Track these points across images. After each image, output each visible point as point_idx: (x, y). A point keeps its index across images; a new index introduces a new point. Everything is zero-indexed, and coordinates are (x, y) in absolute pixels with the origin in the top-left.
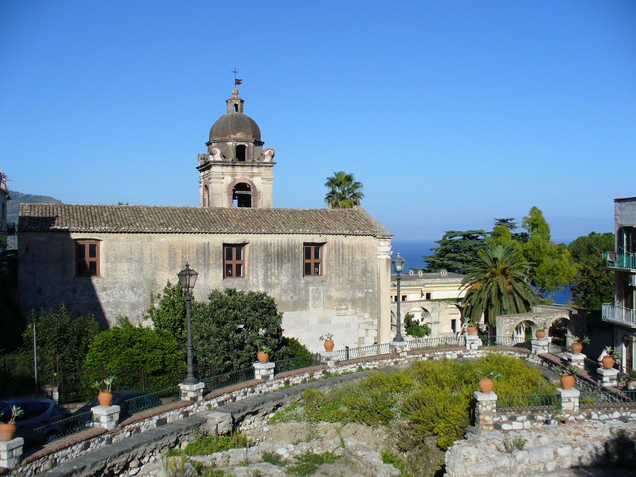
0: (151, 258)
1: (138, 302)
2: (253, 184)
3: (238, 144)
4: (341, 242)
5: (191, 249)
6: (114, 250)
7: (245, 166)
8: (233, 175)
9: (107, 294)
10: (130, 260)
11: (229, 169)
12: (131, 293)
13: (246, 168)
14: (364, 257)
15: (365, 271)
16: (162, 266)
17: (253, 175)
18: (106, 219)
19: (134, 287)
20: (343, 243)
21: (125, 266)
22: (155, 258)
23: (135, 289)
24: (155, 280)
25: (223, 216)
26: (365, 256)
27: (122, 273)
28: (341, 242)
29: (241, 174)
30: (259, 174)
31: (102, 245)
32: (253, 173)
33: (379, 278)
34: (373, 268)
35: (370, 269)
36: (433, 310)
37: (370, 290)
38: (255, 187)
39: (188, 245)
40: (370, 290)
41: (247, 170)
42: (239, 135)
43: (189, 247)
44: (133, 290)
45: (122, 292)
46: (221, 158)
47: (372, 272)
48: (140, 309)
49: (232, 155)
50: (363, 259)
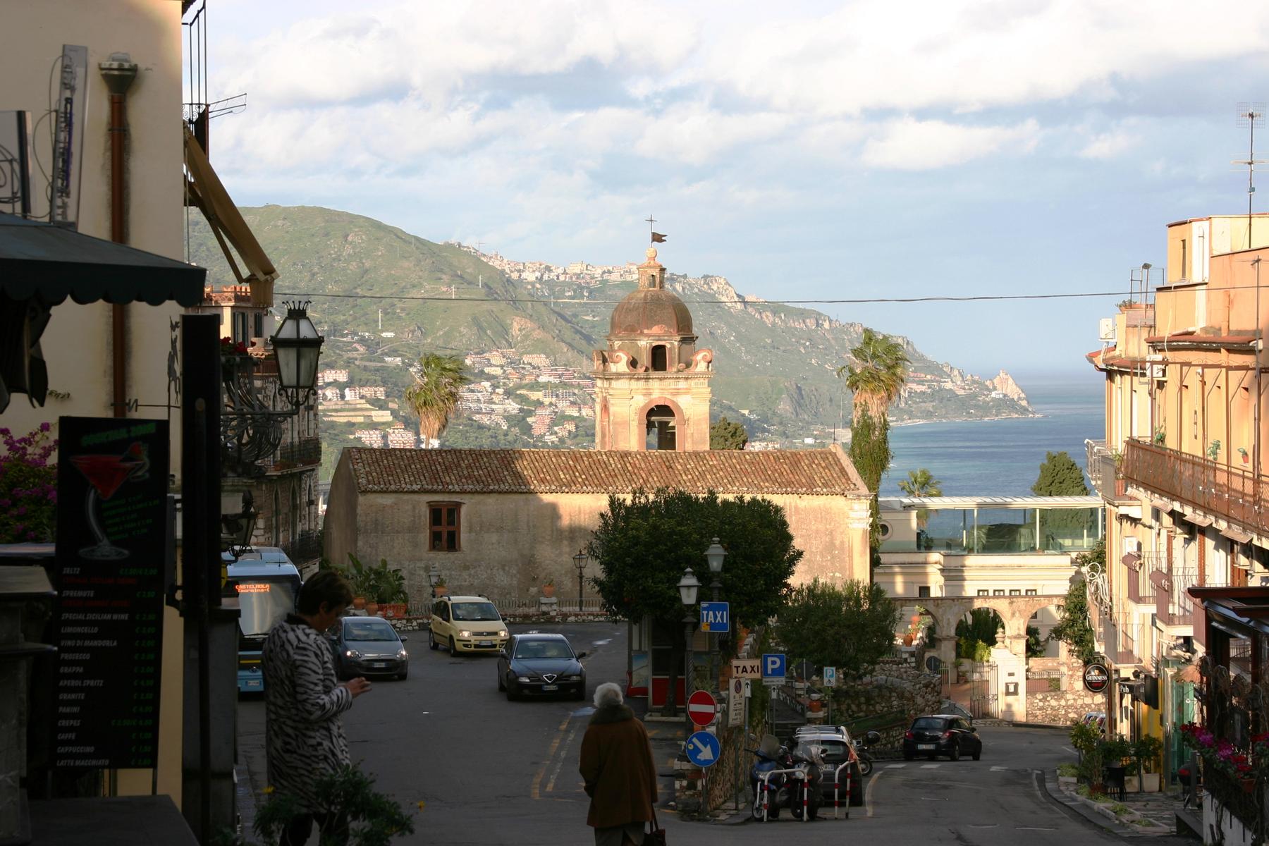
0: (528, 526)
1: (510, 584)
2: (678, 407)
3: (654, 345)
4: (793, 505)
5: (582, 515)
6: (480, 515)
7: (665, 378)
8: (648, 393)
9: (470, 575)
10: (500, 529)
11: (641, 384)
12: (501, 573)
13: (667, 382)
14: (828, 527)
15: (830, 546)
16: (544, 537)
17: (677, 392)
18: (465, 472)
19: (504, 565)
20: (796, 508)
21: (494, 538)
22: (534, 526)
23: (507, 568)
24: (533, 556)
25: (628, 465)
26: (830, 524)
27: (490, 547)
28: (793, 505)
29: (659, 390)
30: (687, 391)
31: (464, 510)
32: (679, 389)
33: (851, 557)
34: (842, 542)
35: (837, 543)
36: (1013, 614)
37: (837, 575)
38: (681, 411)
39: (577, 509)
40: (837, 575)
41: (670, 384)
42: (656, 330)
43: (580, 512)
44: (504, 570)
45: (489, 571)
46: (628, 368)
47: (842, 549)
48: (513, 595)
49: (645, 359)
50: (827, 530)
